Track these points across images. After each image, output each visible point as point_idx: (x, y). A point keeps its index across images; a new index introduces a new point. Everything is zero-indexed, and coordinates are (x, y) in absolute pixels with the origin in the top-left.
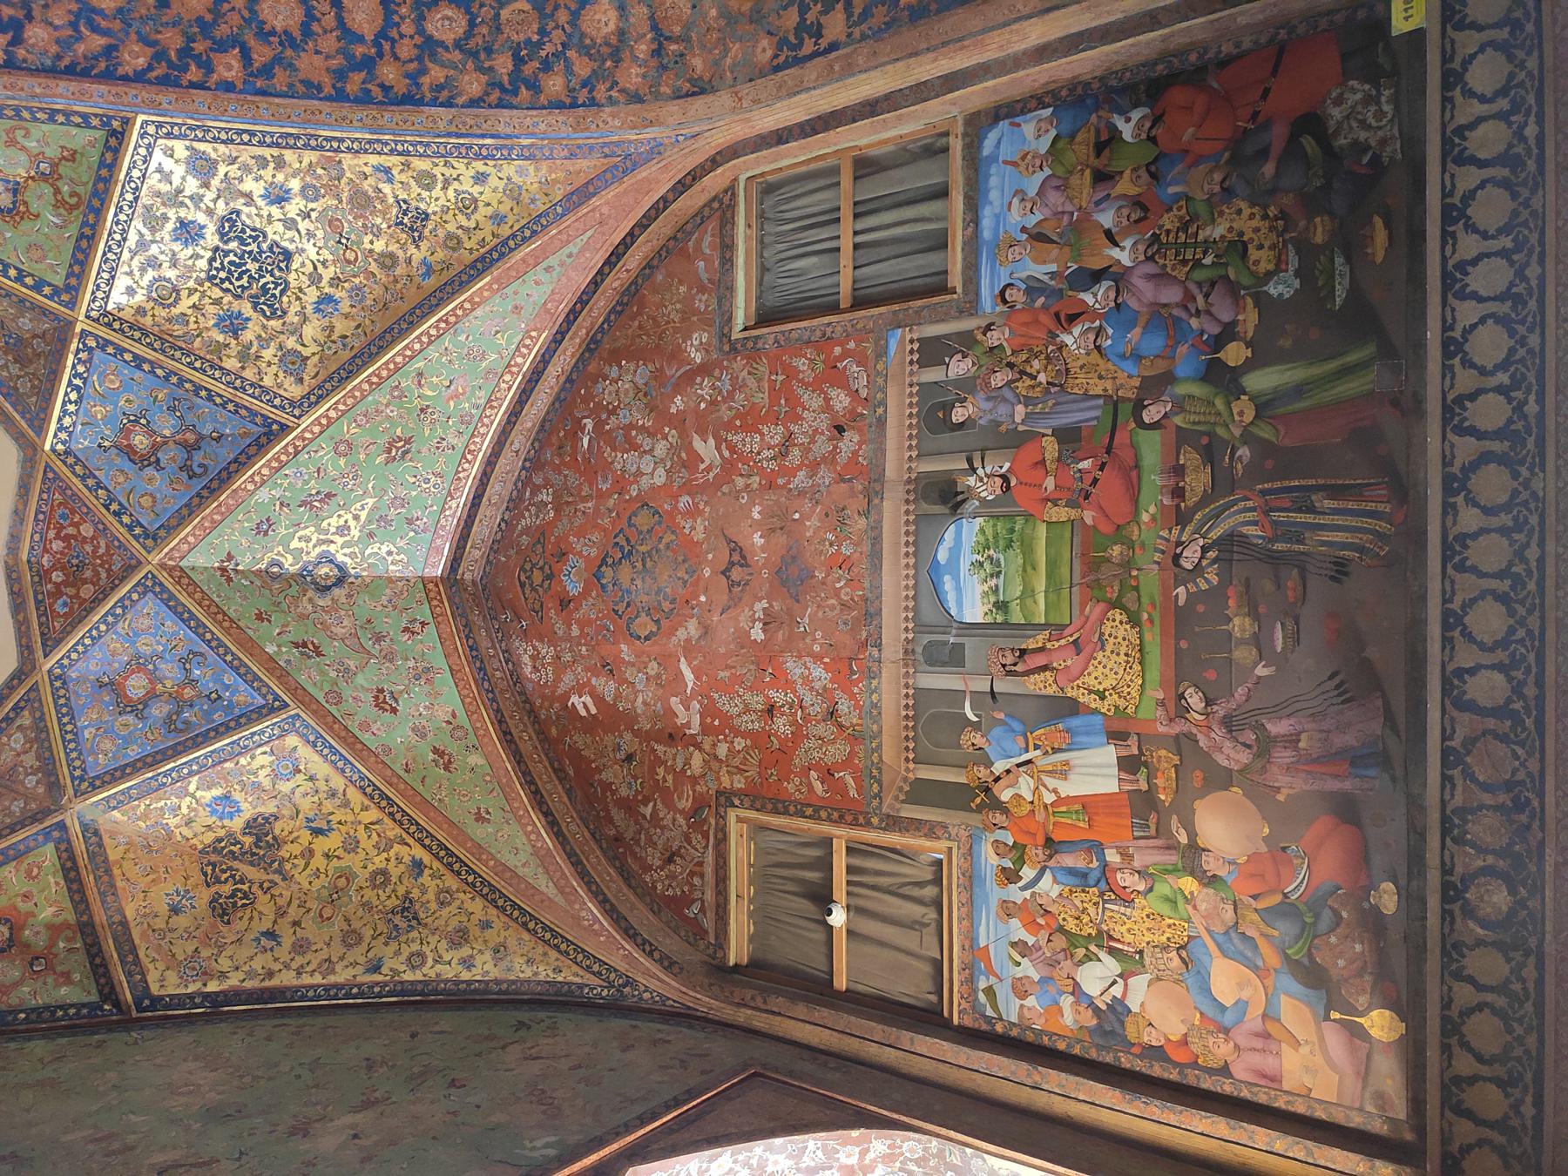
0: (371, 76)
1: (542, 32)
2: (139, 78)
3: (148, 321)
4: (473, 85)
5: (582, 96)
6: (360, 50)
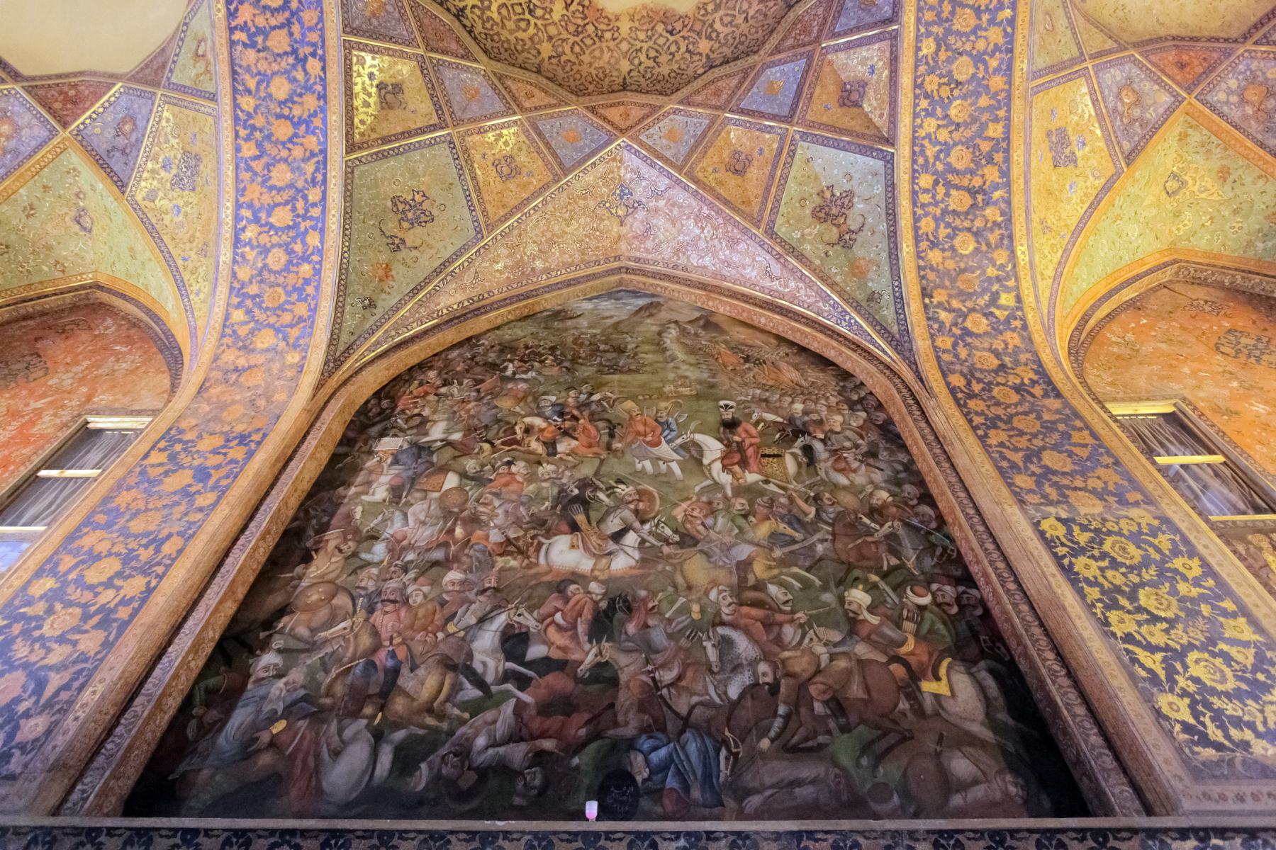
0: (249, 221)
1: (267, 309)
2: (236, 106)
3: (164, 123)
4: (244, 273)
5: (228, 331)
6: (263, 215)
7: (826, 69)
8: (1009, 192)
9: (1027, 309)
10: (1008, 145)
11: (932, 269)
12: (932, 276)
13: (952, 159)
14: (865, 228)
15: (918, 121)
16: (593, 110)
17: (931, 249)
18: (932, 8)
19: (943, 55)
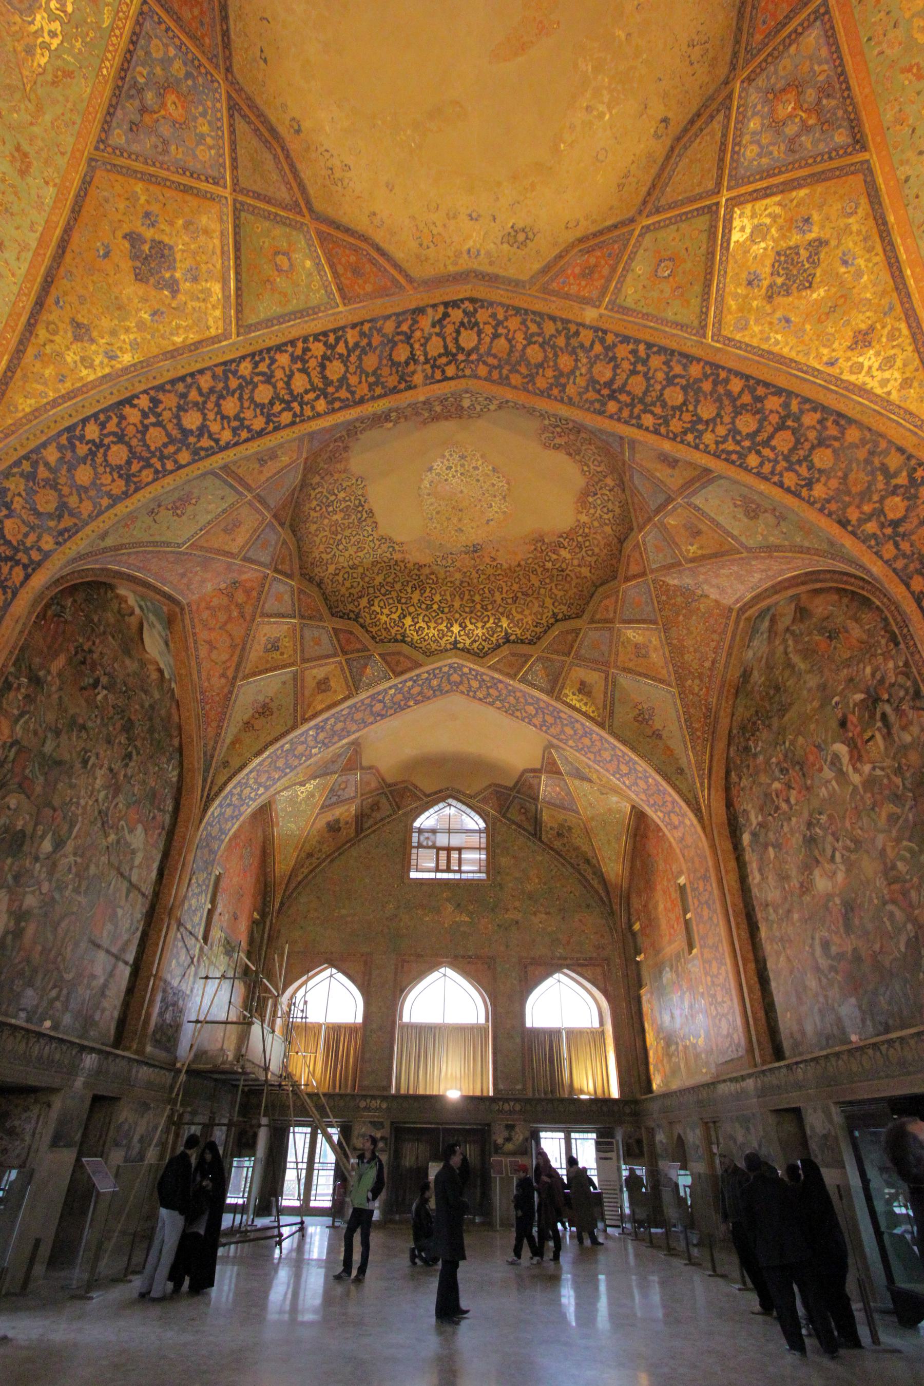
8: (797, 396)
9: (914, 452)
10: (753, 378)
11: (828, 501)
13: (745, 431)
15: (701, 446)
16: (627, 579)
17: (811, 489)
18: (620, 410)
19: (658, 410)
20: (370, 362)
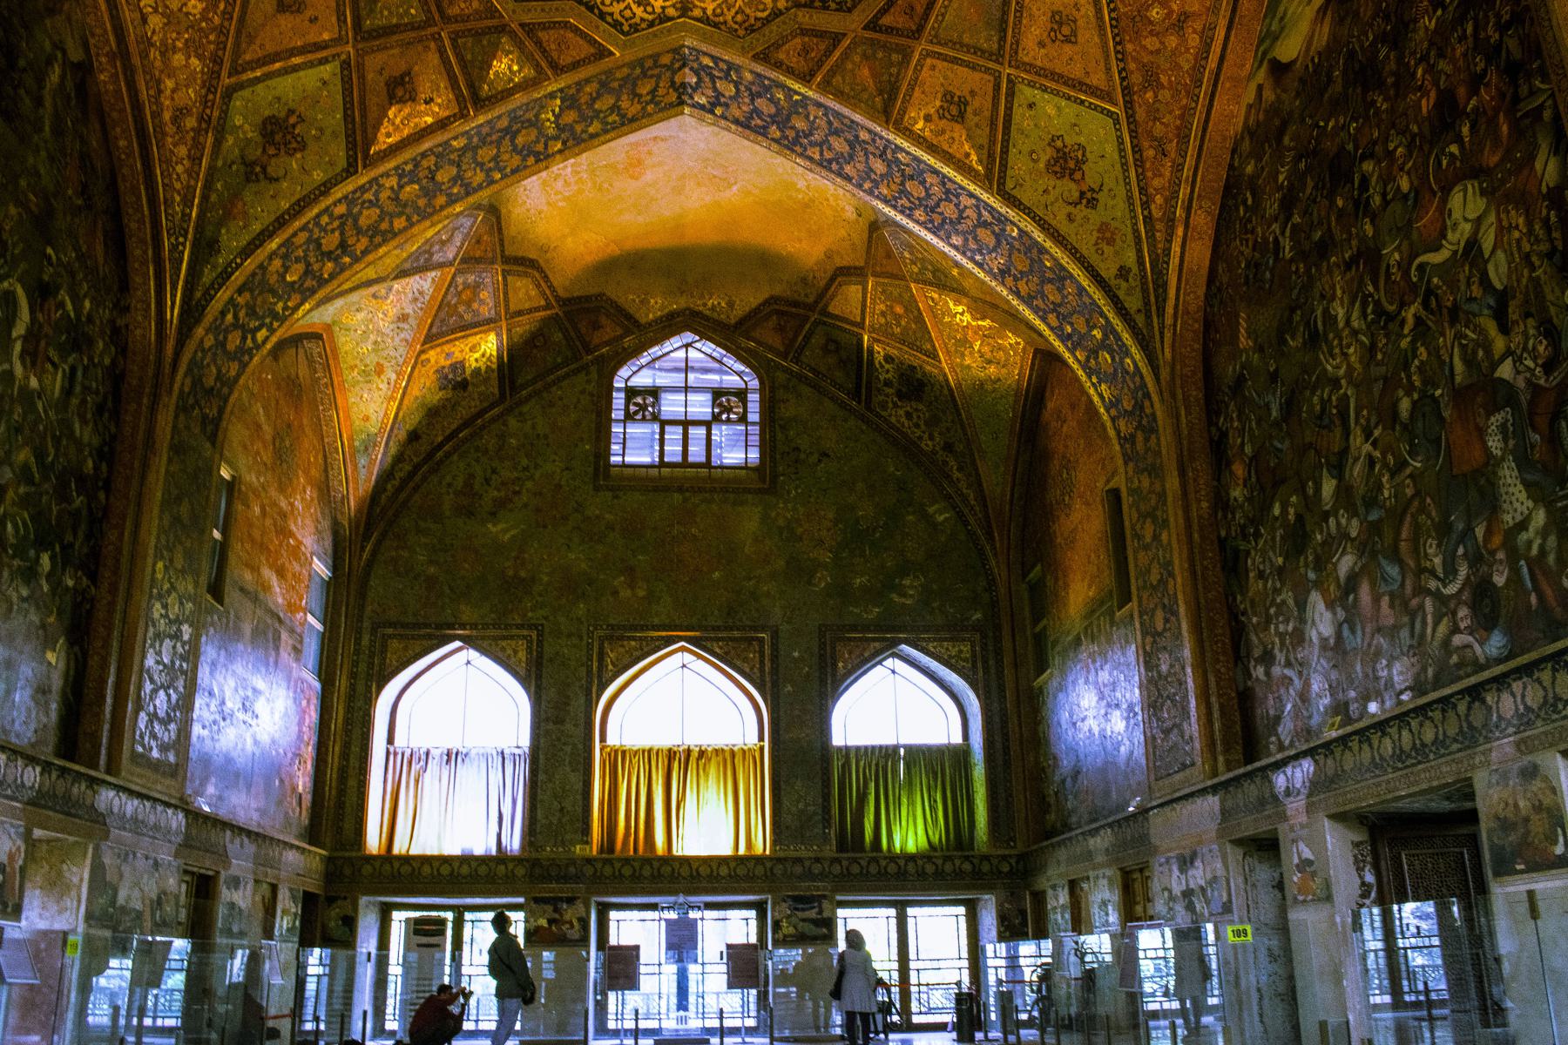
7: (420, 48)
12: (258, 278)
14: (274, 185)
20: (800, 124)
